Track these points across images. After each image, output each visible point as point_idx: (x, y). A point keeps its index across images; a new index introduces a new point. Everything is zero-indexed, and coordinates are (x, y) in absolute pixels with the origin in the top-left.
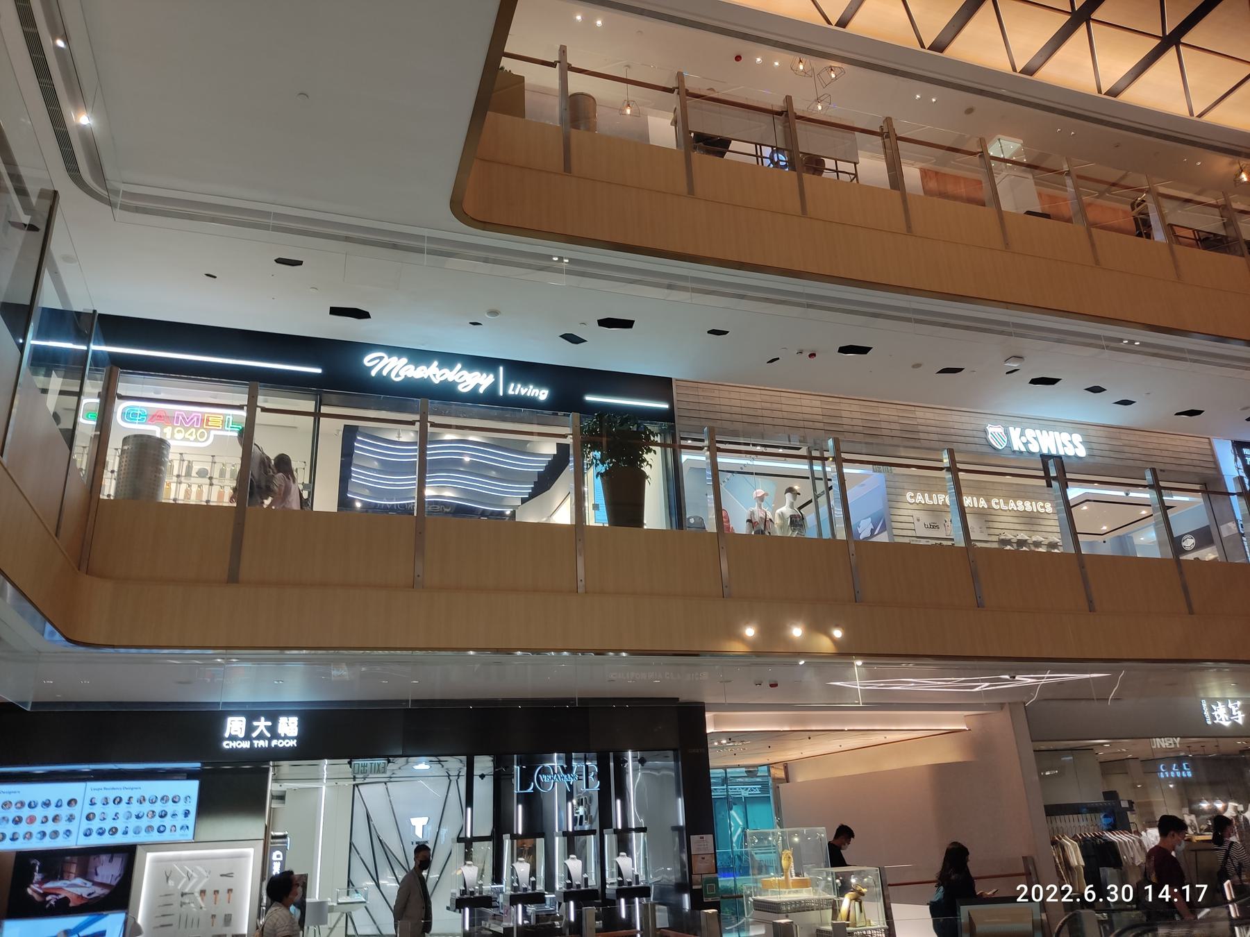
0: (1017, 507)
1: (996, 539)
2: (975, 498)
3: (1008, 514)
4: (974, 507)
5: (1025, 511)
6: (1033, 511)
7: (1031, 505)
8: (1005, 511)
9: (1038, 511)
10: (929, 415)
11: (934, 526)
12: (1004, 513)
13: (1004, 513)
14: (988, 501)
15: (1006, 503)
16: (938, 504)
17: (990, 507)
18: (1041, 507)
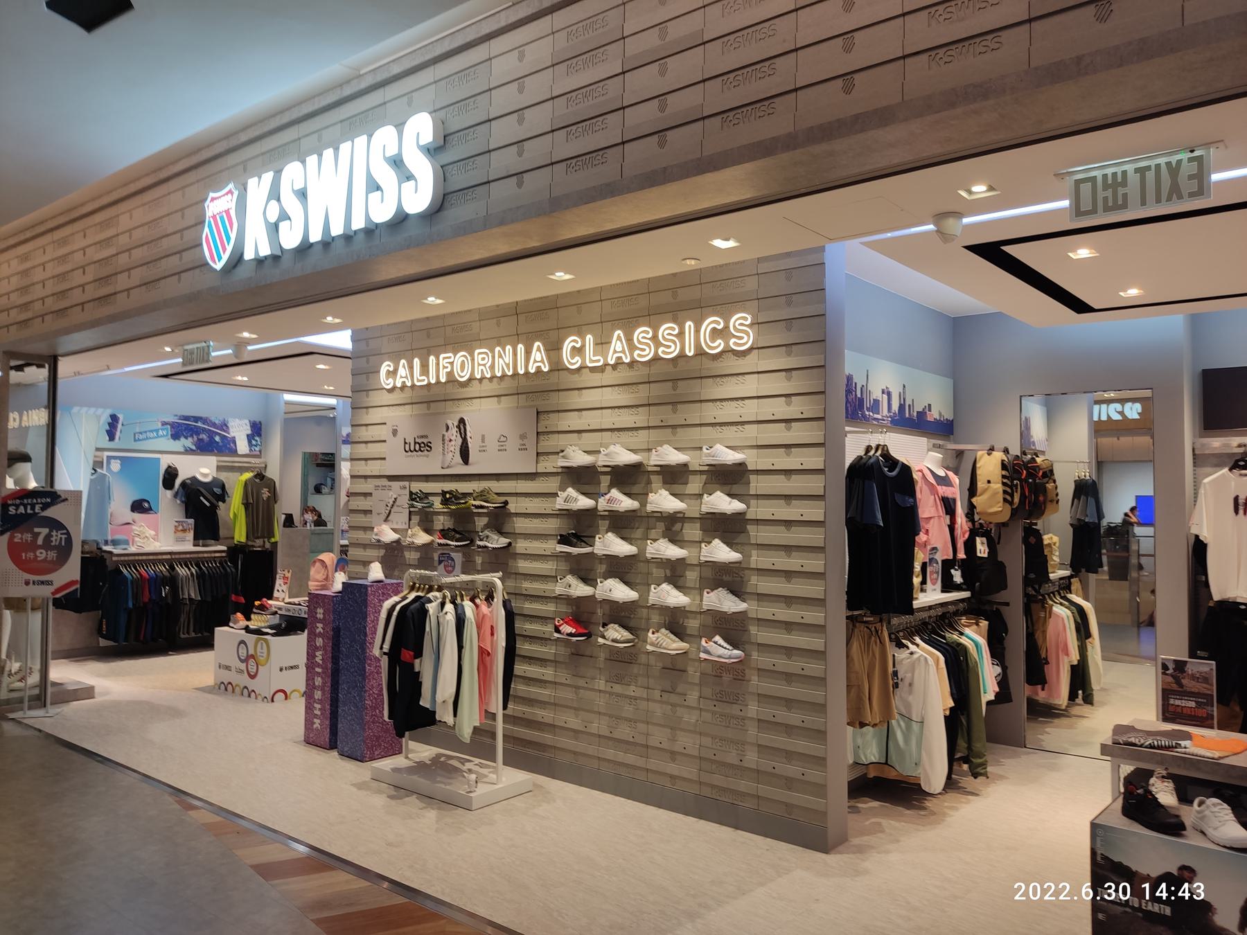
0: (632, 347)
1: (548, 465)
2: (521, 347)
3: (609, 377)
4: (515, 374)
5: (656, 359)
6: (682, 356)
7: (681, 334)
8: (601, 369)
9: (700, 353)
10: (140, 216)
11: (422, 446)
12: (596, 379)
13: (596, 379)
14: (554, 348)
15: (602, 344)
16: (438, 382)
17: (558, 367)
18: (716, 333)
